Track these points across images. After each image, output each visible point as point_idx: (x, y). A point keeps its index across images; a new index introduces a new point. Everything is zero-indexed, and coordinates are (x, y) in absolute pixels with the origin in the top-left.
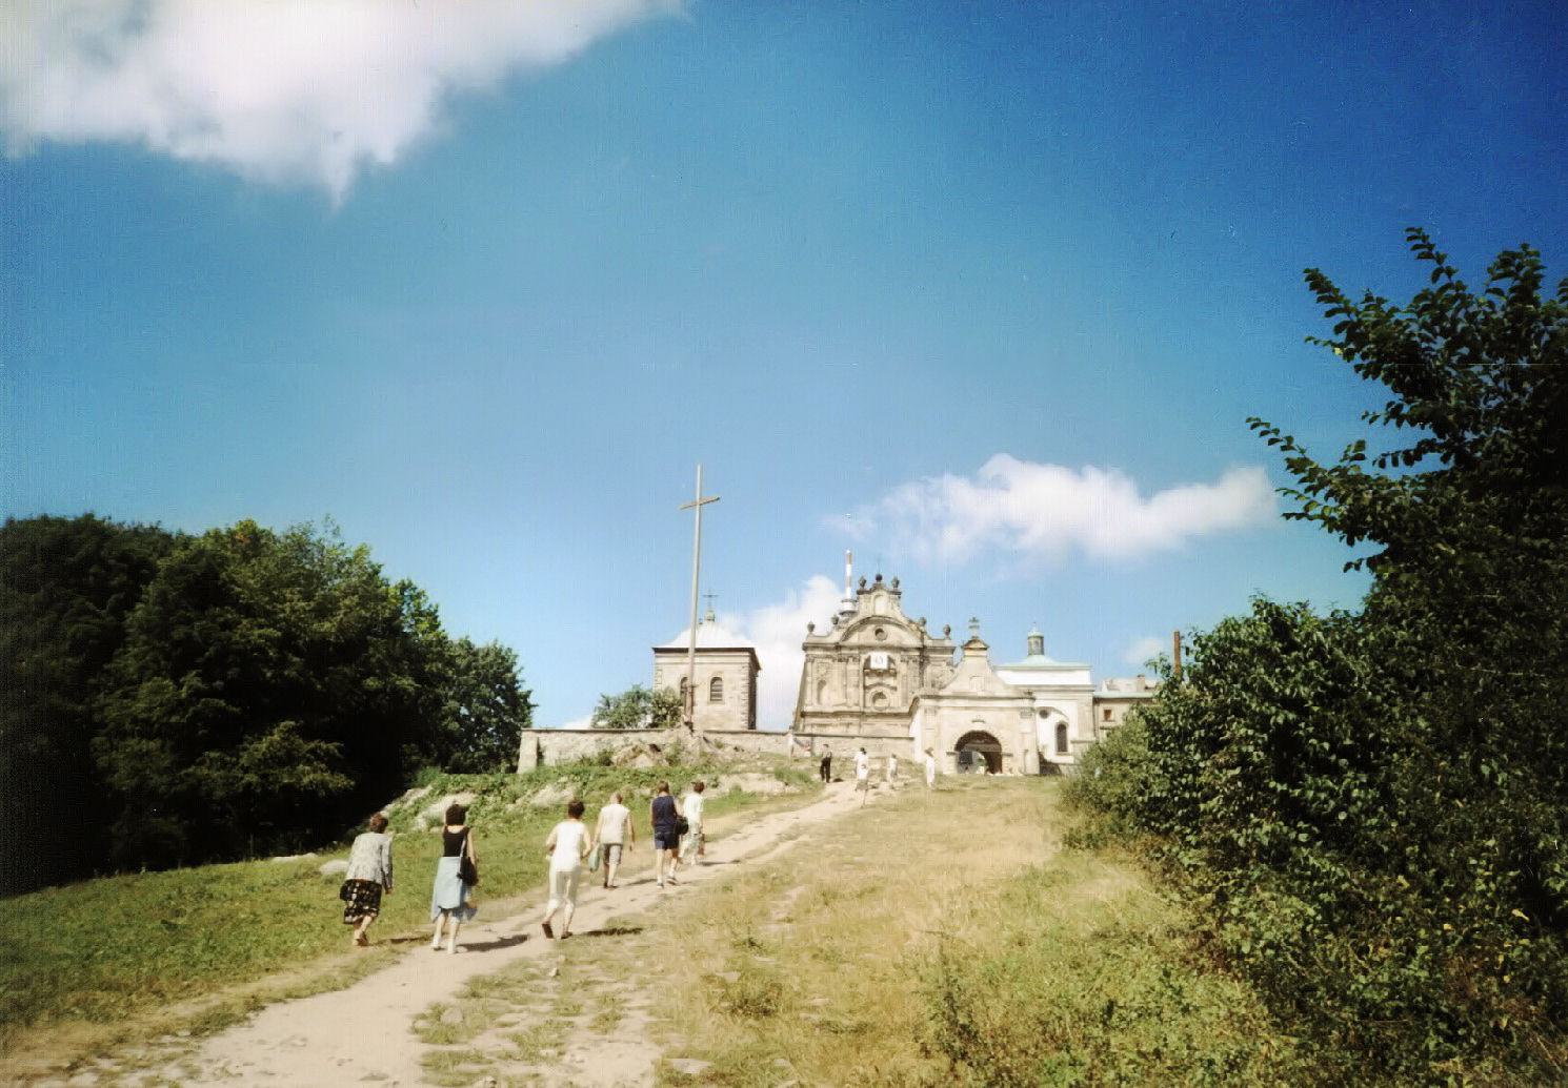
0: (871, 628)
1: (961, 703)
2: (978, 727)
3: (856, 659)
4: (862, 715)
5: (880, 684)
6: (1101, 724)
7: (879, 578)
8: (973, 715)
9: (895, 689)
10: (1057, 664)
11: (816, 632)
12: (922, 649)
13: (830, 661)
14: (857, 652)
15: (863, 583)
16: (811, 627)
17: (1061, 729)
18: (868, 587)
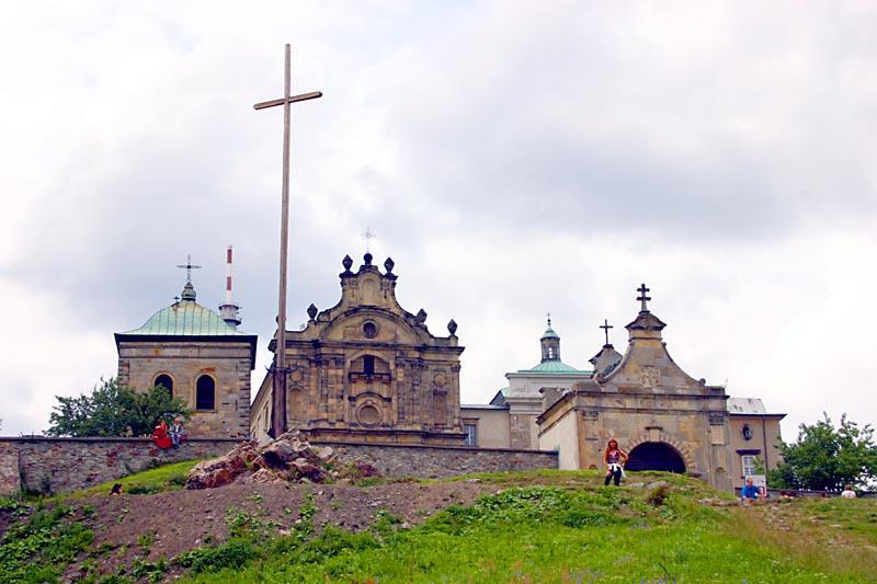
1: (629, 403)
2: (654, 437)
3: (340, 362)
8: (645, 420)
12: (423, 349)
14: (341, 351)
15: (348, 262)
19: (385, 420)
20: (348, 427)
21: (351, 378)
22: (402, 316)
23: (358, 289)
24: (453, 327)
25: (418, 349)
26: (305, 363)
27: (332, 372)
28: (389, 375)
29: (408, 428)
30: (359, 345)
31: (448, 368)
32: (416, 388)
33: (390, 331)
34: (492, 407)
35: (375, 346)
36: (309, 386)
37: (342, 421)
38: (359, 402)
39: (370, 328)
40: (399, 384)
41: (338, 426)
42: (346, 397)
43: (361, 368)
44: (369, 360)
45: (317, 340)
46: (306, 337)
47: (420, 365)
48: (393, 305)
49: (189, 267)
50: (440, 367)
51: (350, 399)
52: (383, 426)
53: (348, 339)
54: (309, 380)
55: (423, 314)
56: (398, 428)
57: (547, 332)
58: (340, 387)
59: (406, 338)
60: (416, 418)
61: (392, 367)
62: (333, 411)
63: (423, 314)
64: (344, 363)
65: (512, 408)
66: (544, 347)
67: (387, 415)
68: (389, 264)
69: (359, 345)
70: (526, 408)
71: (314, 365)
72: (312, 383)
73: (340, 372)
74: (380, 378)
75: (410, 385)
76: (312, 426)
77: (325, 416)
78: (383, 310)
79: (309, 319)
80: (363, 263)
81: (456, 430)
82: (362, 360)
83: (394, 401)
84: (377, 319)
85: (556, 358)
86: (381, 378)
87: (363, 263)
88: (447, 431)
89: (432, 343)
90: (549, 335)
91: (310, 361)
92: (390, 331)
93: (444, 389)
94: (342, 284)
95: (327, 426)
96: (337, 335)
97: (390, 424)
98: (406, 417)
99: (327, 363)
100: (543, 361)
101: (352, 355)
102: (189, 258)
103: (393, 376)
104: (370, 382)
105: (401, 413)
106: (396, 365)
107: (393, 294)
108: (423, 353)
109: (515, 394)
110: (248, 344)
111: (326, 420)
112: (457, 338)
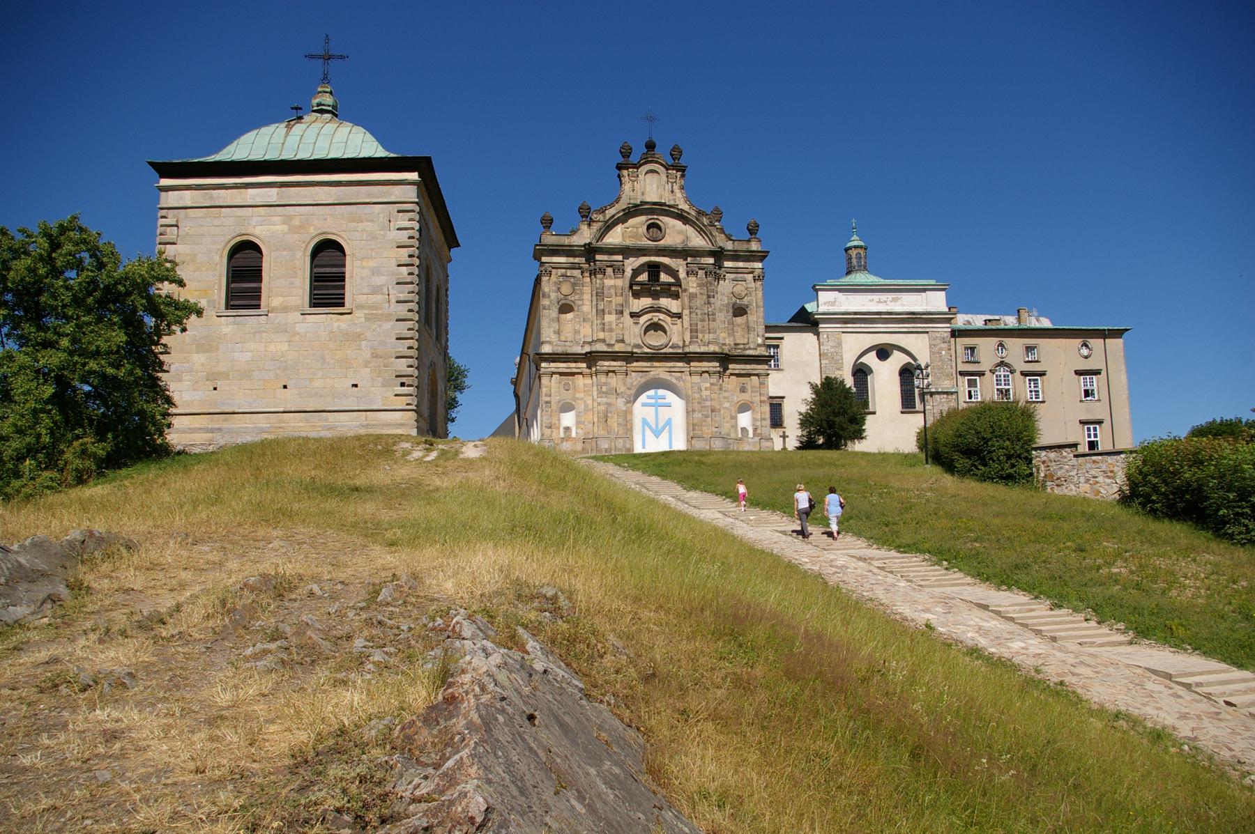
0: (640, 221)
3: (618, 270)
4: (629, 357)
5: (658, 310)
6: (962, 368)
7: (651, 146)
9: (679, 316)
10: (882, 281)
13: (577, 273)
14: (620, 258)
17: (907, 373)
18: (634, 159)
20: (629, 349)
22: (693, 213)
27: (609, 282)
29: (703, 349)
32: (712, 299)
34: (789, 324)
37: (622, 341)
40: (692, 297)
41: (618, 347)
42: (626, 314)
43: (644, 277)
44: (654, 269)
49: (327, 58)
52: (671, 347)
53: (628, 242)
54: (582, 294)
58: (620, 300)
61: (682, 275)
62: (611, 330)
64: (624, 271)
67: (676, 335)
73: (619, 282)
75: (705, 297)
76: (587, 349)
77: (601, 335)
81: (762, 351)
83: (686, 318)
84: (661, 218)
92: (680, 232)
93: (746, 301)
95: (605, 349)
97: (681, 344)
98: (700, 336)
101: (632, 263)
102: (327, 39)
104: (655, 295)
105: (694, 331)
106: (688, 273)
110: (414, 176)
111: (603, 341)
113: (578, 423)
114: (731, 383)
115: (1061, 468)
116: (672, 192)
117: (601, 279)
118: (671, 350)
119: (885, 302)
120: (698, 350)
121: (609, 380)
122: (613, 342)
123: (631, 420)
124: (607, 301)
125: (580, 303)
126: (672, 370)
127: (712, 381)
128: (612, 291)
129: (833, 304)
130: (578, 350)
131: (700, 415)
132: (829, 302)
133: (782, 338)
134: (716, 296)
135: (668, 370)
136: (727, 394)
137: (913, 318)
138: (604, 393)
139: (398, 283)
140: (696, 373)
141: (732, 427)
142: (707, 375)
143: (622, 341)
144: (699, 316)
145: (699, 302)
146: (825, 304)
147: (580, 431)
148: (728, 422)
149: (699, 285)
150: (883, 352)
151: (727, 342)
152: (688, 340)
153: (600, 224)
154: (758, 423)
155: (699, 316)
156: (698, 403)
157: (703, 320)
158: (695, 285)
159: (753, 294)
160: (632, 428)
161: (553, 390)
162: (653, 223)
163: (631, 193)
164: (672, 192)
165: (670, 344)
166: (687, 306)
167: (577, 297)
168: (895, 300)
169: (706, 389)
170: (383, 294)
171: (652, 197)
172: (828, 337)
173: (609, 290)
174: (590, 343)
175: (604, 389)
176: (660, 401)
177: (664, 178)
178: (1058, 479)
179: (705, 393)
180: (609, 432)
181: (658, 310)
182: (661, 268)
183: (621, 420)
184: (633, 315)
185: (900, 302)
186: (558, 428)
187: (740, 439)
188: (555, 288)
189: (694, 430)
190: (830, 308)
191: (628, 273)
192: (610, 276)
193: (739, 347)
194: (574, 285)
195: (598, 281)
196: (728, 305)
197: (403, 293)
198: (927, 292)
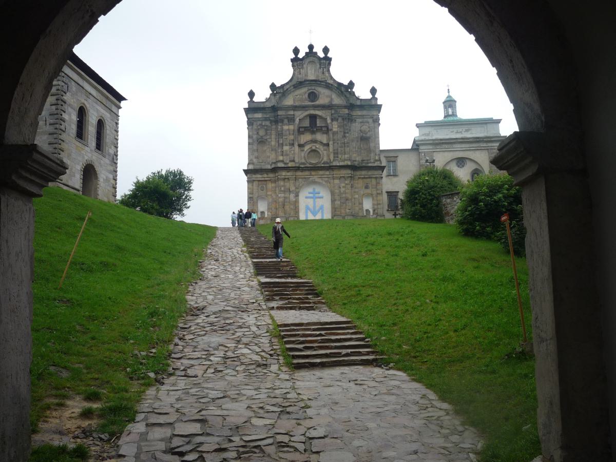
0: (304, 91)
3: (291, 120)
5: (315, 141)
11: (256, 99)
14: (291, 113)
15: (296, 51)
16: (251, 94)
19: (325, 159)
20: (297, 165)
21: (301, 131)
23: (303, 68)
24: (373, 91)
25: (345, 107)
26: (268, 123)
27: (286, 127)
28: (327, 127)
29: (342, 164)
30: (304, 108)
31: (370, 120)
32: (347, 135)
33: (327, 96)
35: (316, 107)
36: (271, 138)
37: (293, 161)
38: (307, 148)
39: (313, 96)
40: (334, 133)
41: (290, 165)
43: (307, 123)
44: (313, 118)
45: (274, 106)
46: (269, 105)
47: (350, 119)
48: (329, 78)
50: (365, 120)
51: (300, 146)
52: (323, 164)
53: (297, 104)
54: (271, 134)
55: (351, 84)
56: (334, 164)
57: (447, 97)
59: (337, 101)
60: (346, 156)
61: (329, 121)
62: (287, 155)
63: (351, 84)
64: (294, 121)
65: (421, 147)
66: (445, 107)
67: (326, 156)
68: (326, 50)
69: (304, 108)
70: (431, 147)
71: (274, 124)
72: (273, 136)
73: (291, 127)
74: (320, 129)
75: (342, 133)
76: (273, 166)
77: (281, 158)
78: (321, 82)
79: (271, 92)
80: (308, 51)
82: (308, 118)
83: (331, 146)
85: (454, 115)
86: (321, 129)
87: (308, 51)
88: (370, 165)
89: (358, 103)
90: (449, 99)
91: (271, 122)
92: (327, 96)
93: (368, 135)
94: (293, 66)
96: (289, 101)
97: (328, 161)
98: (340, 156)
99: (282, 121)
100: (445, 117)
101: (300, 115)
103: (330, 128)
104: (313, 133)
105: (336, 154)
106: (332, 120)
107: (329, 71)
108: (352, 110)
109: (423, 138)
111: (282, 161)
112: (377, 99)
113: (269, 209)
114: (360, 184)
115: (453, 208)
116: (323, 73)
117: (281, 126)
118: (323, 165)
119: (461, 132)
120: (338, 165)
121: (286, 184)
122: (288, 162)
123: (299, 206)
124: (285, 138)
125: (270, 140)
126: (323, 176)
127: (346, 182)
128: (288, 132)
129: (428, 135)
130: (269, 167)
131: (339, 203)
132: (425, 134)
133: (397, 157)
134: (350, 133)
135: (320, 176)
136: (357, 190)
137: (477, 140)
138: (282, 191)
139: (50, 115)
140: (337, 178)
141: (360, 209)
142: (343, 179)
143: (293, 161)
144: (339, 145)
145: (340, 135)
146: (423, 135)
147: (270, 214)
148: (357, 206)
149: (338, 127)
150: (461, 162)
151: (357, 159)
152: (332, 159)
153: (280, 94)
154: (376, 207)
155: (339, 145)
156: (338, 195)
157: (341, 147)
158: (336, 126)
159: (373, 130)
160: (299, 211)
161: (254, 191)
162: (312, 92)
163: (299, 76)
164: (323, 73)
165: (322, 162)
166: (332, 139)
167: (268, 137)
168: (467, 131)
169: (343, 187)
170: (43, 121)
171: (311, 77)
172: (425, 155)
173: (286, 131)
174: (275, 163)
175: (282, 189)
176: (317, 195)
177: (318, 66)
178: (451, 215)
179: (342, 190)
180: (285, 214)
181: (315, 141)
182: (318, 117)
183: (292, 207)
184: (300, 146)
185: (470, 132)
186: (257, 212)
187: (365, 216)
188: (256, 133)
189: (335, 211)
190: (426, 137)
191: (297, 120)
192: (286, 124)
193: (364, 162)
194: (266, 130)
195: (279, 127)
196: (357, 138)
197: (53, 119)
198: (488, 125)
